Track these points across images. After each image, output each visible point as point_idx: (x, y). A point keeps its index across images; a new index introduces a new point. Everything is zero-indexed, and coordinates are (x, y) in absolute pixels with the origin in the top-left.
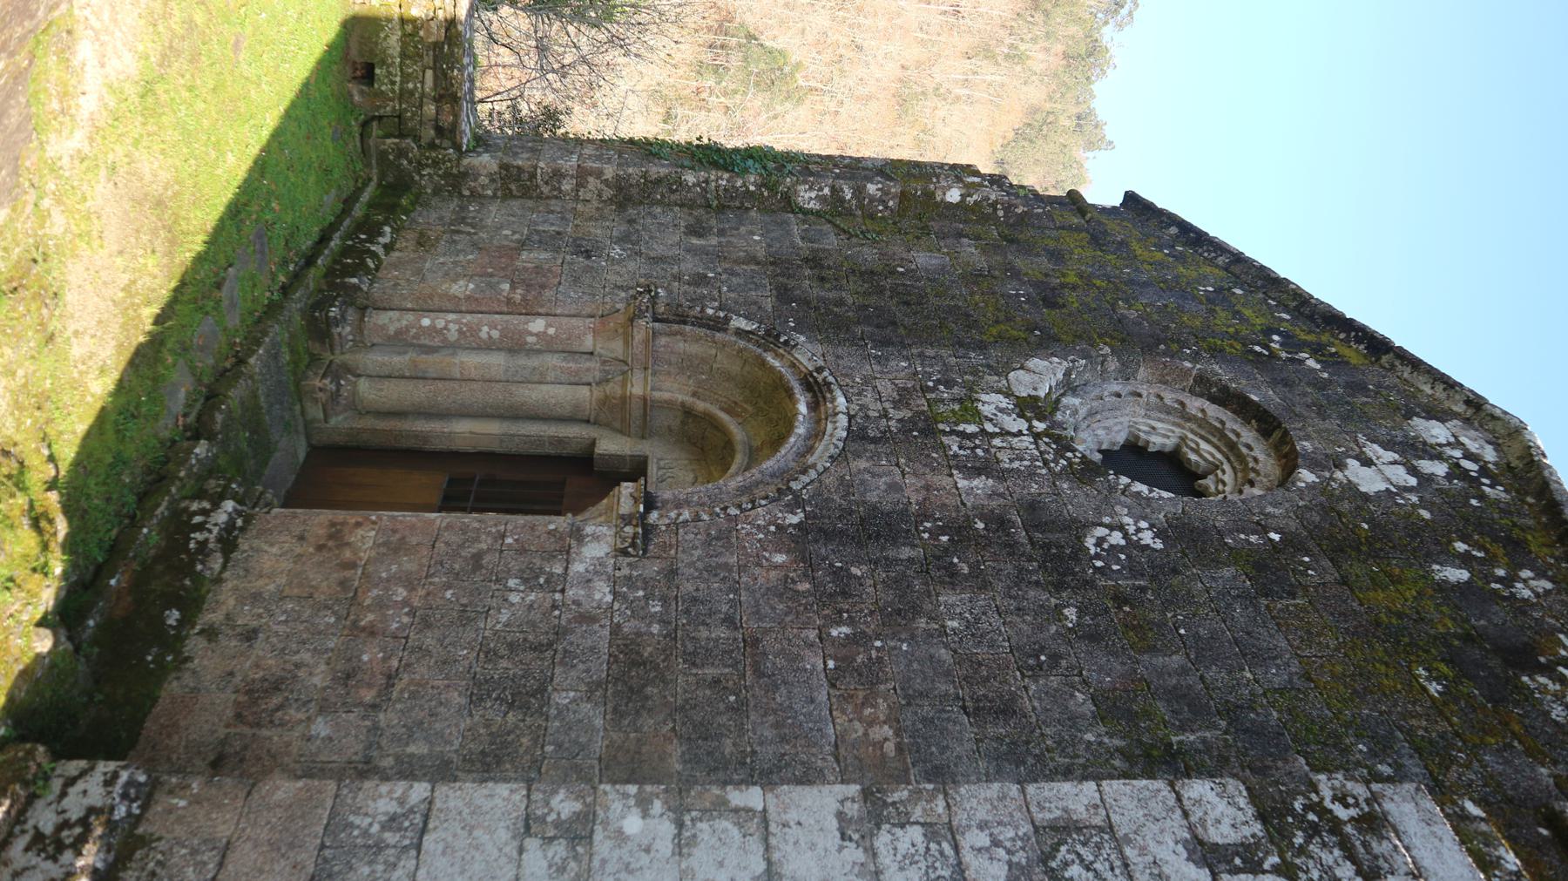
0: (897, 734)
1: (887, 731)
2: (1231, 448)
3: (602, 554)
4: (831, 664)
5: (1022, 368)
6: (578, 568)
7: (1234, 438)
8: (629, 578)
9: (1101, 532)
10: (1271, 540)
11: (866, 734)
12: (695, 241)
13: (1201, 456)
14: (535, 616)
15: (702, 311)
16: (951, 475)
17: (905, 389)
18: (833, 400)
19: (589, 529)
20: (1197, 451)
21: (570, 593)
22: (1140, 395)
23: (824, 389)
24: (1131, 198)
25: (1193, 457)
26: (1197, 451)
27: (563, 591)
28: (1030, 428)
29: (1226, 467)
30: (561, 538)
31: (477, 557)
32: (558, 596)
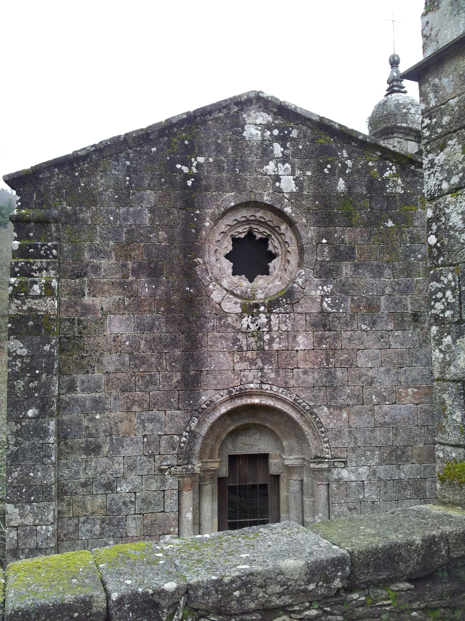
0: (411, 387)
1: (409, 390)
2: (248, 221)
3: (346, 471)
4: (387, 403)
5: (219, 304)
6: (353, 478)
7: (245, 219)
8: (356, 462)
9: (325, 304)
10: (326, 243)
11: (411, 396)
12: (106, 449)
13: (243, 232)
14: (374, 488)
15: (184, 442)
16: (297, 351)
17: (241, 358)
18: (252, 388)
19: (336, 477)
20: (240, 233)
21: (364, 479)
22: (217, 250)
23: (243, 391)
24: (14, 180)
25: (242, 236)
26: (240, 233)
27: (363, 481)
28: (263, 313)
29: (254, 226)
30: (340, 485)
31: (350, 509)
32: (365, 482)
